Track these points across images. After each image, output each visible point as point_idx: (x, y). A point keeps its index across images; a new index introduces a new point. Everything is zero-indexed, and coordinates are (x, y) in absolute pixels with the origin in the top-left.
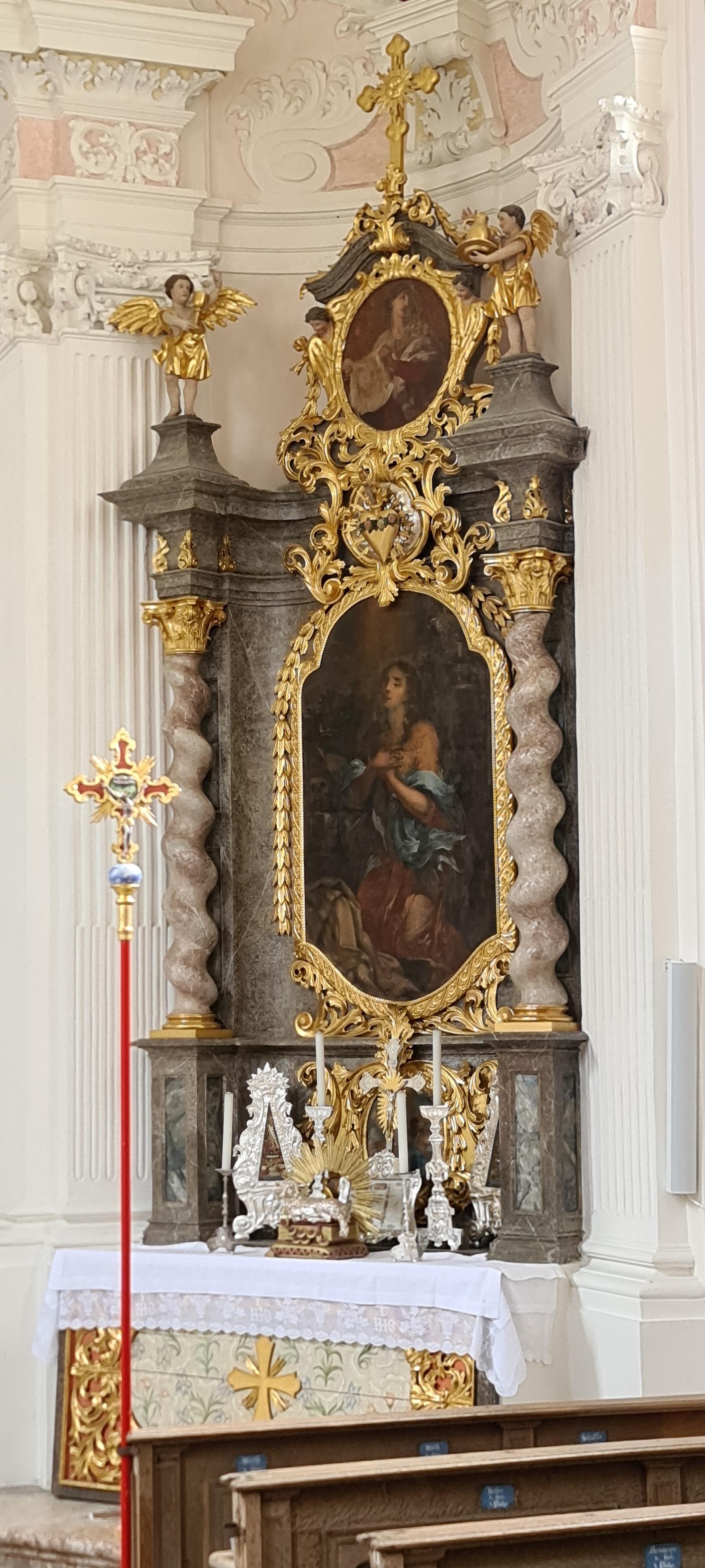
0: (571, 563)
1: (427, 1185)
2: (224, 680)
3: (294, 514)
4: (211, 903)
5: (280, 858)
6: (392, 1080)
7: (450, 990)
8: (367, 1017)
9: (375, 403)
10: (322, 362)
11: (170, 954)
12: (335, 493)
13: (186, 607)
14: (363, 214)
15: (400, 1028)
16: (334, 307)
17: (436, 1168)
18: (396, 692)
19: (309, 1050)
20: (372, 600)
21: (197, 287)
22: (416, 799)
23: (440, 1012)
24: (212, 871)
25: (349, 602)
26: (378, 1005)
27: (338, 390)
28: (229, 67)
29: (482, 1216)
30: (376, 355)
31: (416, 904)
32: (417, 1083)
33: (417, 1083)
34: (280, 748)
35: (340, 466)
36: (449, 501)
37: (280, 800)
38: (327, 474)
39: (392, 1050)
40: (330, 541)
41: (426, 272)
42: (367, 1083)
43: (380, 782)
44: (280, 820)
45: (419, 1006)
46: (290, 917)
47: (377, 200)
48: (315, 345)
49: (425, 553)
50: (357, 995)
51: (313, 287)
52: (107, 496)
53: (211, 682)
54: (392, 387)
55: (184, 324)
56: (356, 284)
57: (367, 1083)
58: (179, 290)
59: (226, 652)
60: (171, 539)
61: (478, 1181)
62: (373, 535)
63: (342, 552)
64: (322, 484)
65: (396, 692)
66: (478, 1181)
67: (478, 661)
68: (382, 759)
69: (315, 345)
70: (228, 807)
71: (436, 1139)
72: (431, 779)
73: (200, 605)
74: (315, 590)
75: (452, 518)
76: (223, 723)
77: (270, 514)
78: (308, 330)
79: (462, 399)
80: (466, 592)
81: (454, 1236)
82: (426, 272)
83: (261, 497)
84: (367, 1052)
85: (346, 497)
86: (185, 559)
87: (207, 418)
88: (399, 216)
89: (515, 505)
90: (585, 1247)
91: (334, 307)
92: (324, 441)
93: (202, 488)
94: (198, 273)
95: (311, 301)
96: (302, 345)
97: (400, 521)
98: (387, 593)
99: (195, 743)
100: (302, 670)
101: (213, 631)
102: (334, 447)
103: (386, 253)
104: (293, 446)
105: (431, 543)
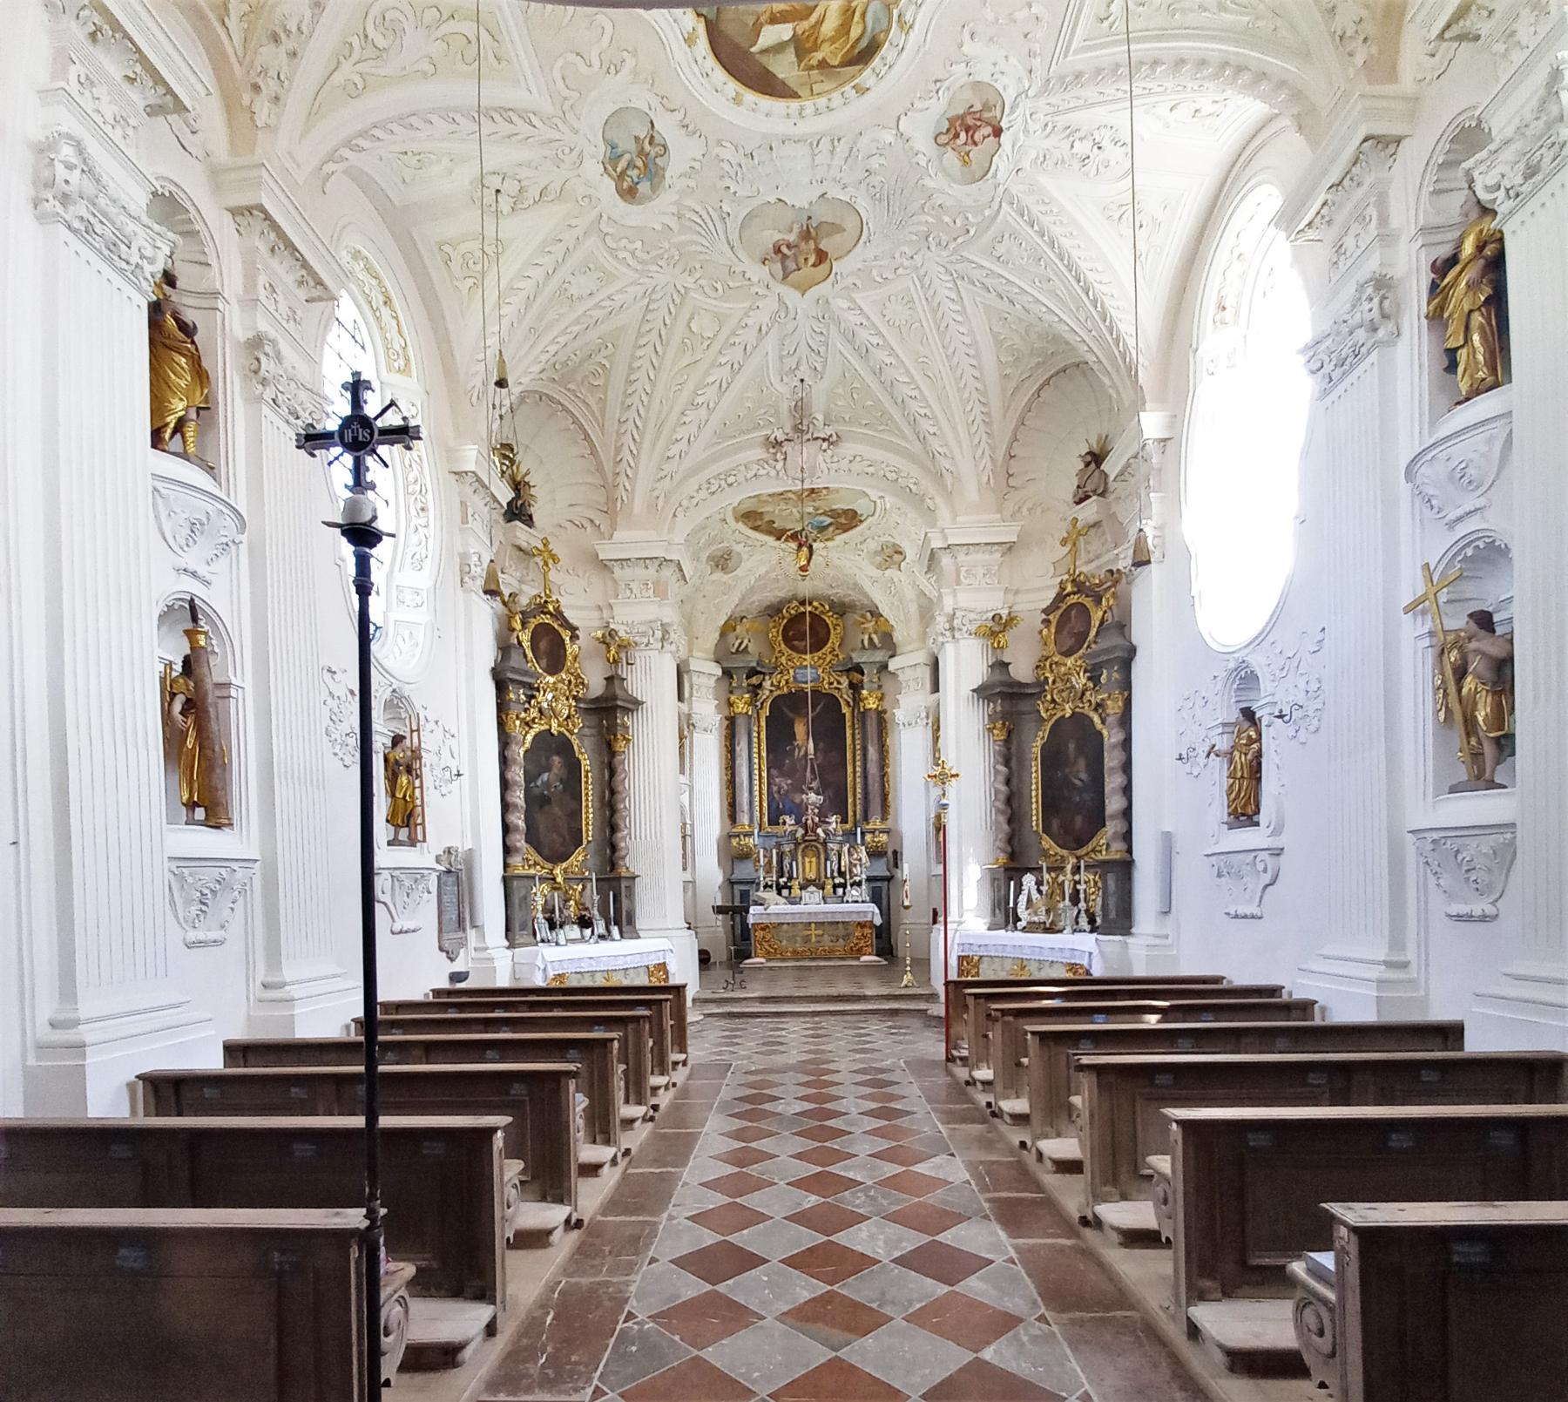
0: (1130, 695)
1: (1079, 911)
2: (1013, 748)
3: (1037, 690)
4: (1010, 822)
5: (1034, 806)
6: (1069, 876)
7: (1090, 846)
8: (1062, 857)
9: (1064, 649)
10: (1048, 636)
11: (995, 841)
12: (1050, 681)
13: (999, 724)
14: (1061, 582)
15: (1072, 860)
16: (1051, 617)
17: (1082, 905)
18: (1072, 746)
19: (1040, 869)
20: (1063, 716)
21: (1004, 617)
22: (1077, 782)
23: (1087, 854)
24: (1009, 811)
25: (1055, 718)
26: (1065, 852)
27: (1053, 645)
28: (1014, 539)
29: (1099, 921)
30: (1065, 632)
31: (1079, 821)
32: (1077, 877)
33: (1077, 877)
34: (1034, 769)
35: (1052, 671)
36: (1089, 679)
37: (1034, 787)
38: (1047, 675)
39: (1069, 867)
40: (1049, 697)
41: (1083, 600)
42: (1061, 878)
43: (1066, 778)
44: (1034, 793)
45: (1080, 852)
46: (1037, 825)
47: (1066, 577)
48: (1045, 632)
49: (1081, 698)
50: (1058, 850)
51: (1044, 611)
52: (974, 691)
53: (1009, 749)
54: (1070, 642)
55: (997, 629)
56: (1058, 608)
57: (1061, 878)
58: (997, 618)
59: (1014, 737)
60: (995, 703)
61: (1098, 910)
62: (1064, 694)
63: (1053, 701)
64: (1046, 679)
65: (1072, 746)
66: (1098, 910)
67: (1100, 734)
68: (1067, 770)
69: (1045, 632)
70: (1015, 789)
71: (1082, 896)
72: (1083, 776)
73: (1004, 724)
74: (1044, 715)
75: (1091, 684)
76: (1013, 763)
77: (1030, 691)
78: (1042, 626)
79: (1095, 642)
80: (1096, 710)
81: (1088, 928)
82: (1083, 600)
83: (1027, 685)
84: (1061, 869)
85: (1054, 682)
86: (999, 708)
87: (1006, 660)
88: (1074, 581)
89: (1109, 677)
90: (1133, 930)
91: (1051, 617)
92: (1048, 664)
93: (1003, 684)
94: (1004, 613)
95: (1044, 616)
96: (1041, 632)
97: (1073, 687)
98: (1068, 713)
99: (1002, 768)
100: (1039, 743)
101: (1009, 732)
102: (1051, 666)
103: (1069, 595)
104: (1037, 667)
105: (1083, 694)
